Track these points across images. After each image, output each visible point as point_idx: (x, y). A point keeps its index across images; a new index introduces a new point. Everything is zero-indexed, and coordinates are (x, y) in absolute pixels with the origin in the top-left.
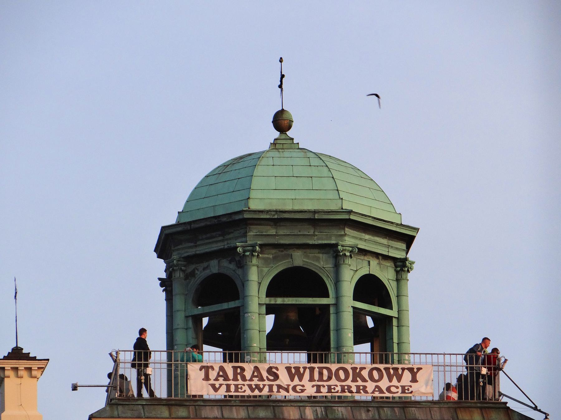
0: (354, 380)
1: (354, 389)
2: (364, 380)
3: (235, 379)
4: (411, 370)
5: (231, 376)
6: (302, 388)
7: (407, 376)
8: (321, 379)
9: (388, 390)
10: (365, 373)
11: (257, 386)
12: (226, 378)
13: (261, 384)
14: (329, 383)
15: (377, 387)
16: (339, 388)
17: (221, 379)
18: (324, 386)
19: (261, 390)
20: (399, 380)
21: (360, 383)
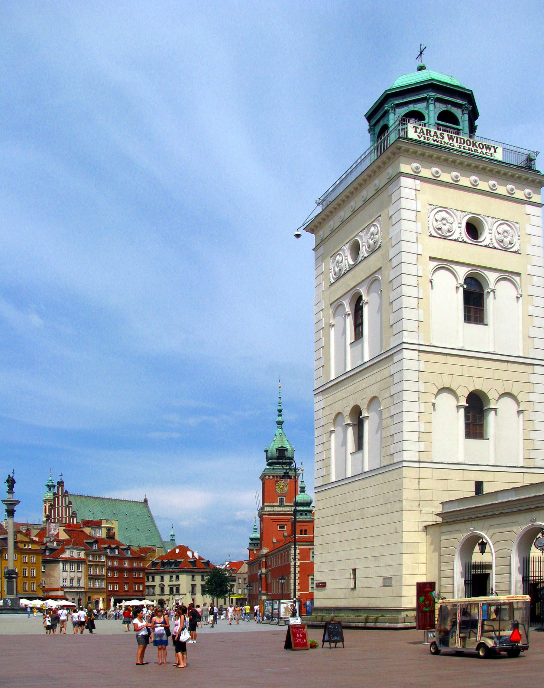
0: (473, 146)
2: (477, 147)
3: (427, 135)
5: (425, 133)
7: (492, 150)
8: (460, 143)
9: (486, 153)
10: (477, 144)
12: (424, 134)
13: (438, 139)
16: (467, 148)
17: (421, 134)
19: (437, 142)
20: (490, 150)
21: (475, 148)
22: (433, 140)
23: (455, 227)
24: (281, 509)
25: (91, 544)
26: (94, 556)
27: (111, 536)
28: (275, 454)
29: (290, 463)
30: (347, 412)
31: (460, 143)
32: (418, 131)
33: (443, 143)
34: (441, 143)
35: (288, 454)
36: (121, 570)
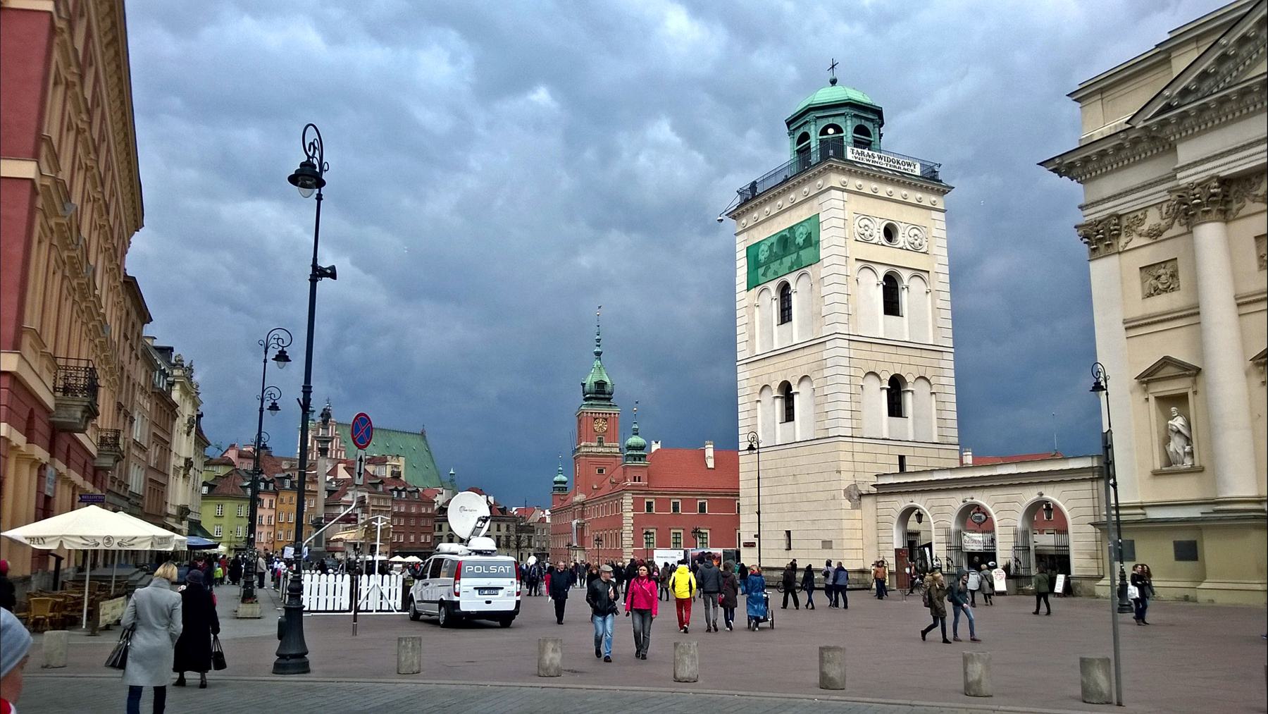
23: (875, 231)
24: (600, 449)
25: (375, 485)
26: (378, 499)
27: (396, 476)
28: (594, 389)
29: (609, 399)
30: (775, 386)
35: (608, 389)
36: (407, 516)
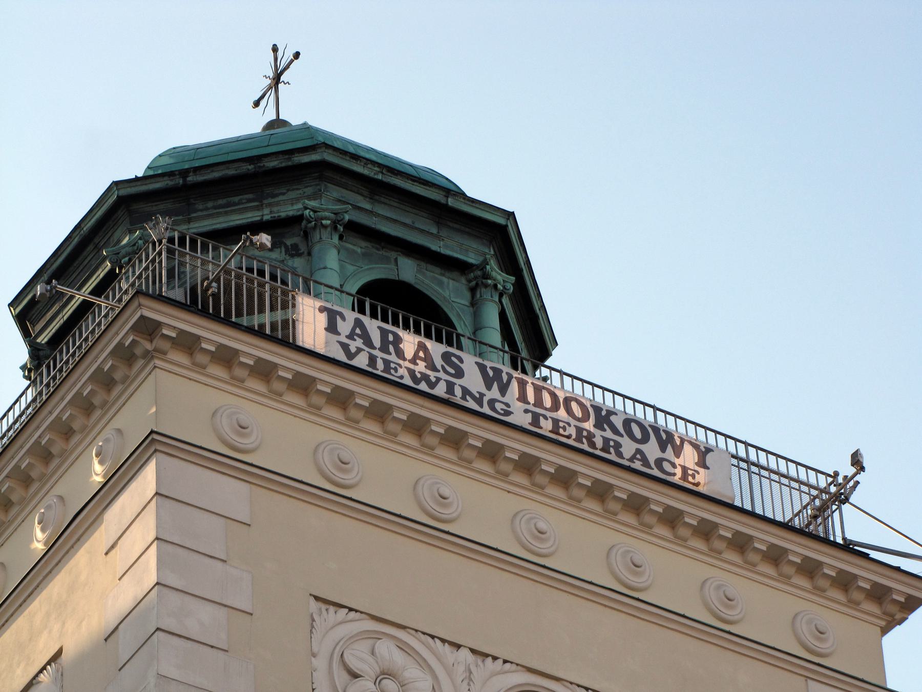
1: (599, 442)
2: (615, 431)
3: (384, 349)
4: (695, 446)
5: (377, 342)
6: (505, 408)
9: (659, 462)
10: (618, 421)
11: (425, 378)
12: (369, 343)
13: (432, 375)
14: (554, 415)
15: (638, 451)
16: (572, 431)
17: (359, 343)
18: (546, 418)
21: (609, 434)
22: (412, 373)
31: (539, 402)
32: (345, 327)
33: (458, 392)
34: (450, 387)
